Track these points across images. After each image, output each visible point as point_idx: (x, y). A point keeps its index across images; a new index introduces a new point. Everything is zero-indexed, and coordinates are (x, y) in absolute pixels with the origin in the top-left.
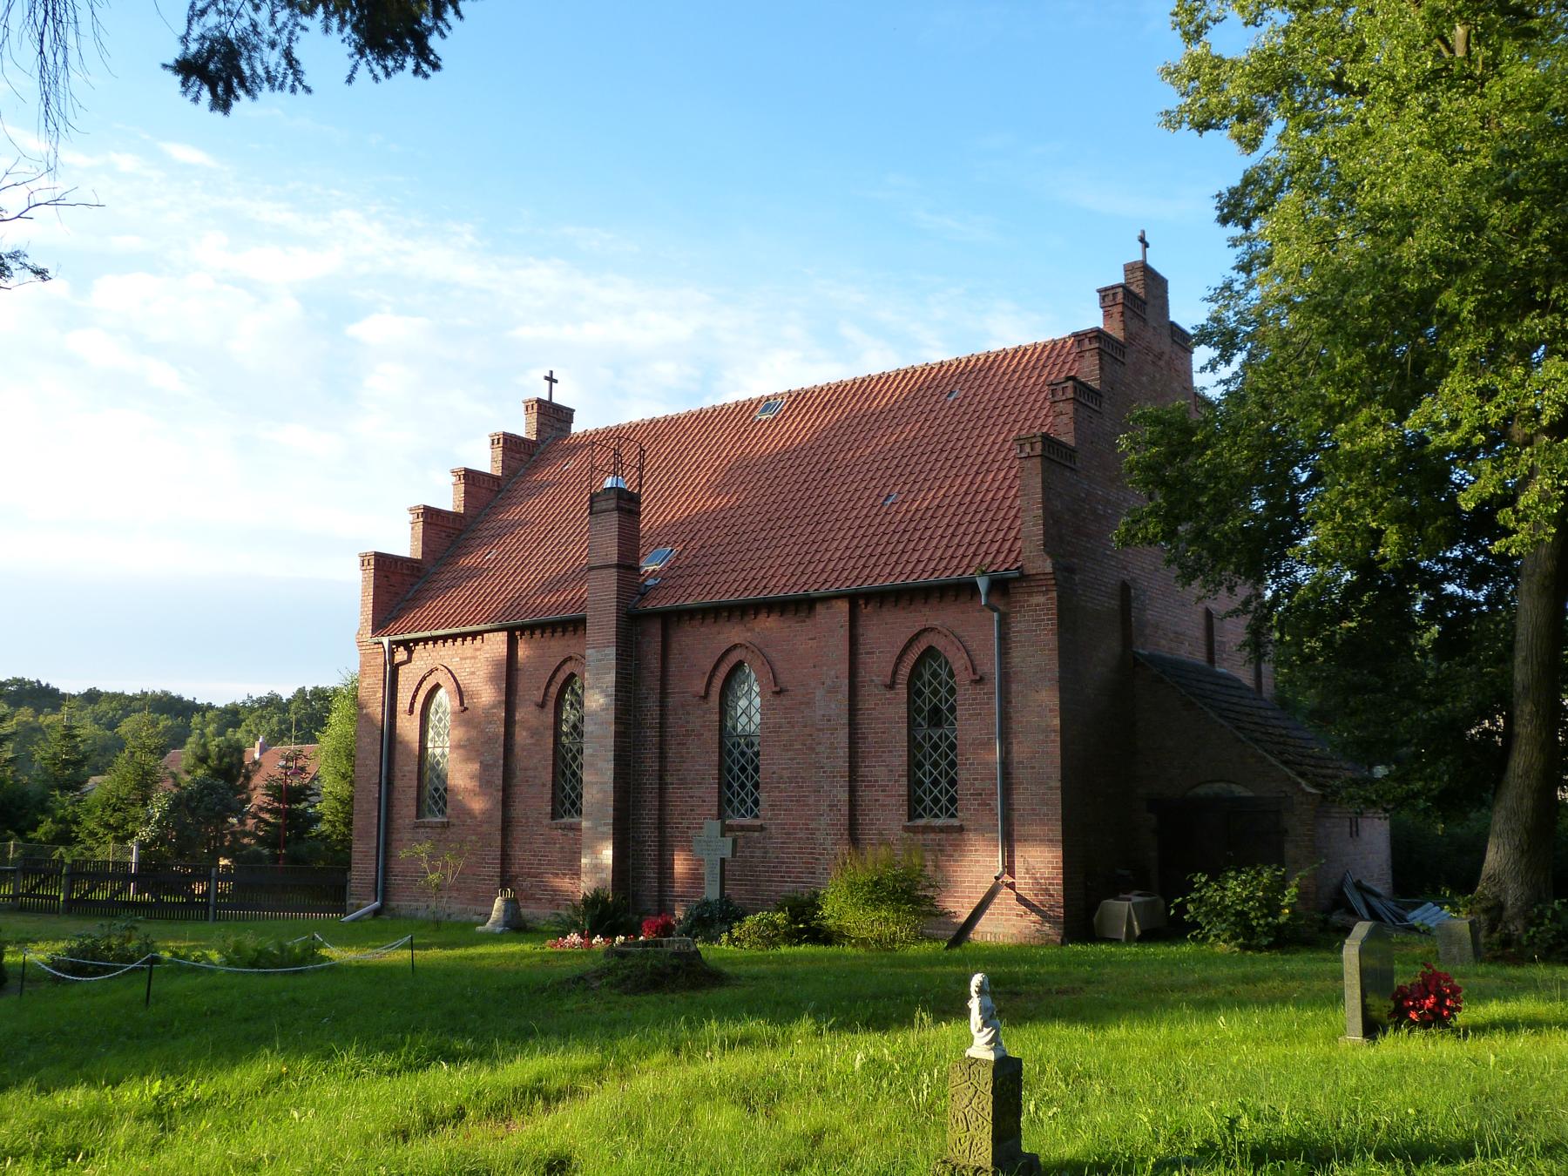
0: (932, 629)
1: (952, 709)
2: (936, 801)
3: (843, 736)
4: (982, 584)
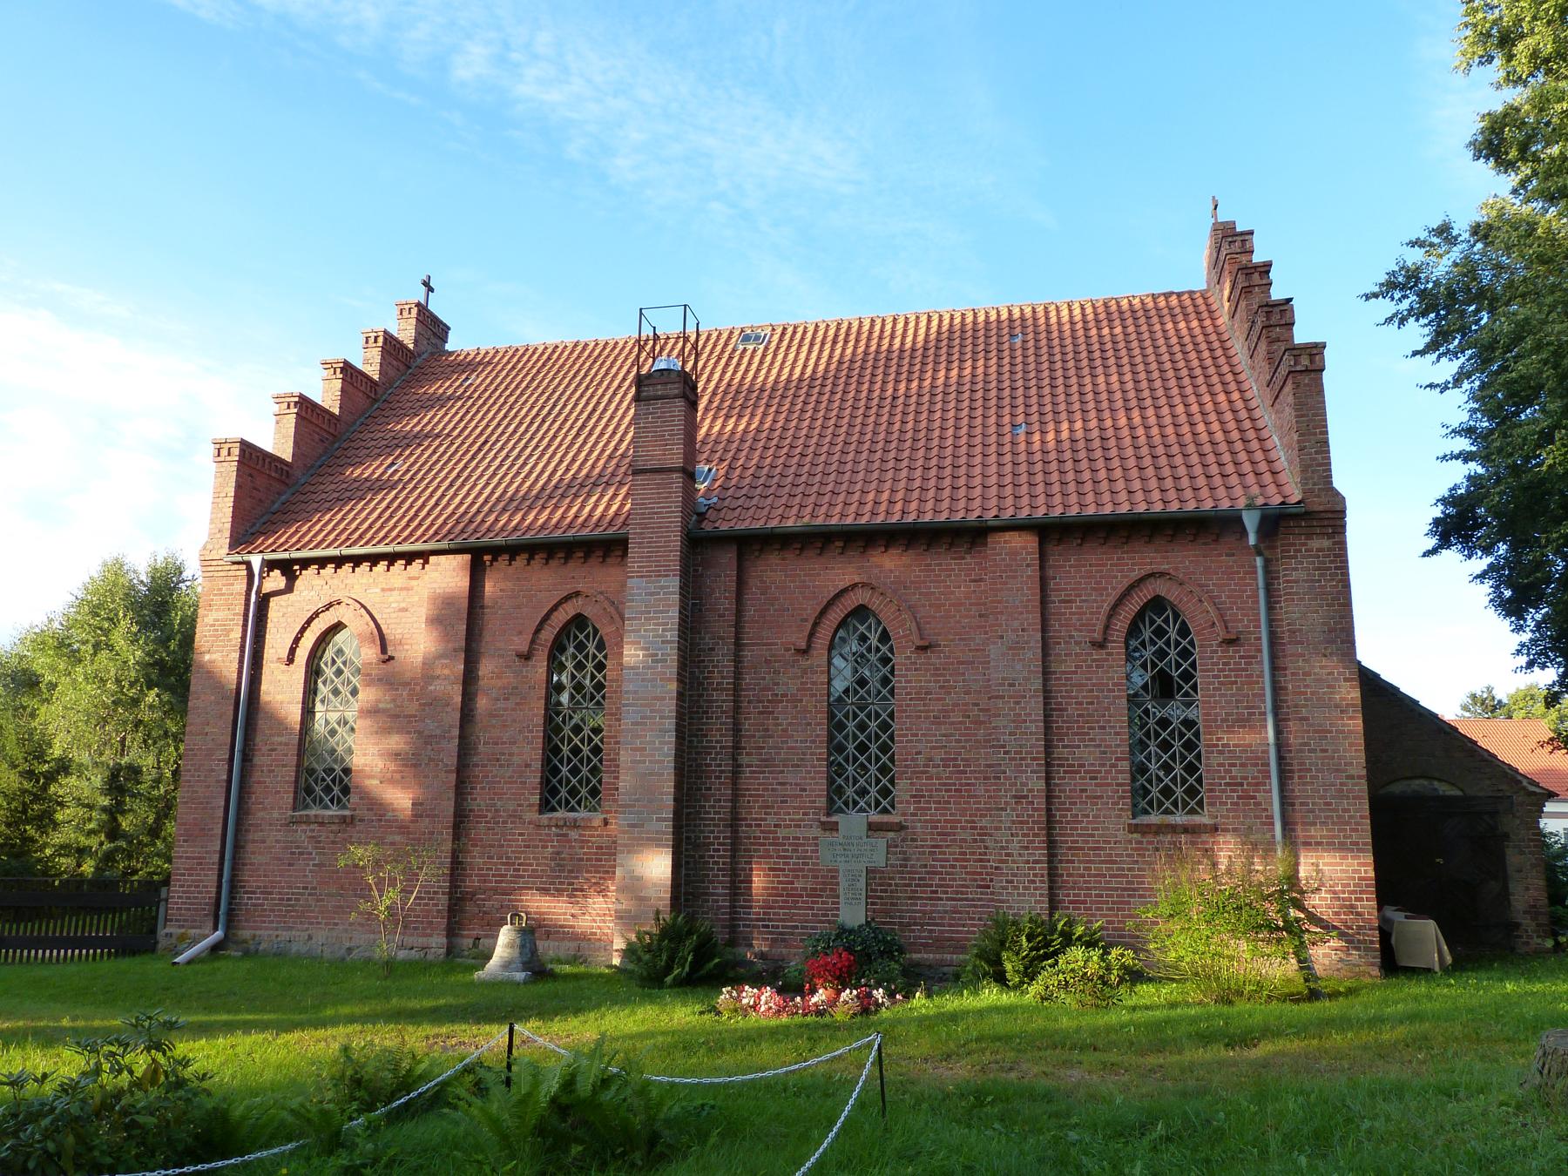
0: (1162, 574)
1: (1187, 676)
2: (1167, 792)
3: (1035, 707)
4: (1251, 521)
